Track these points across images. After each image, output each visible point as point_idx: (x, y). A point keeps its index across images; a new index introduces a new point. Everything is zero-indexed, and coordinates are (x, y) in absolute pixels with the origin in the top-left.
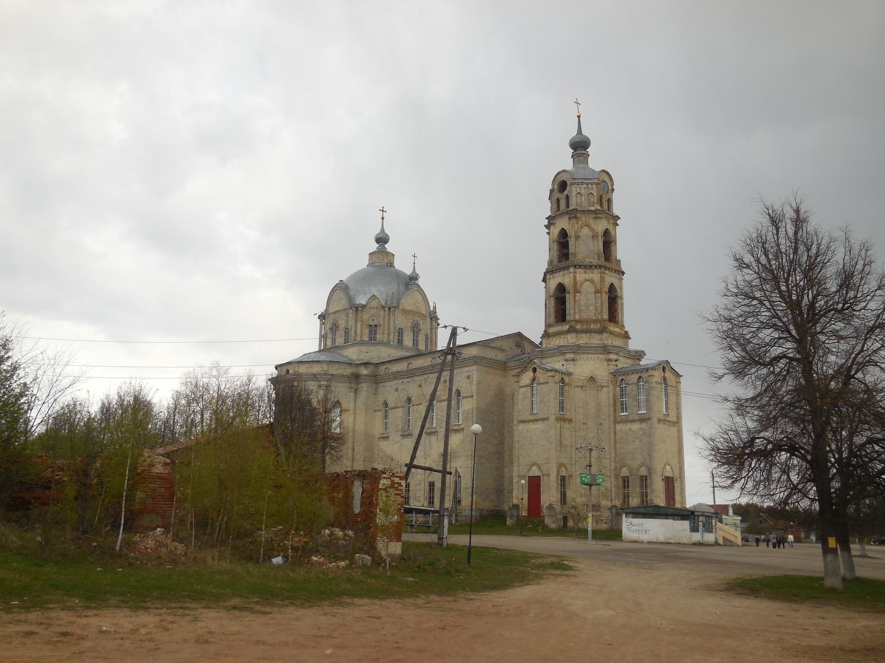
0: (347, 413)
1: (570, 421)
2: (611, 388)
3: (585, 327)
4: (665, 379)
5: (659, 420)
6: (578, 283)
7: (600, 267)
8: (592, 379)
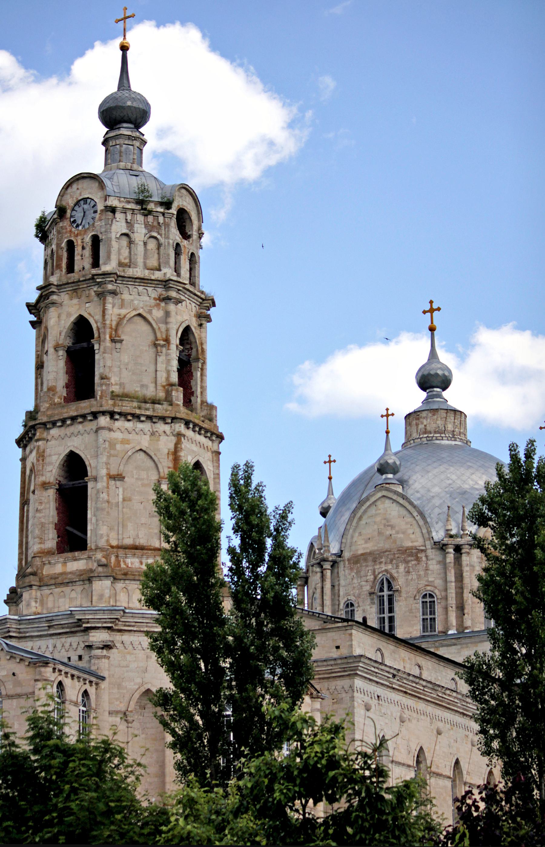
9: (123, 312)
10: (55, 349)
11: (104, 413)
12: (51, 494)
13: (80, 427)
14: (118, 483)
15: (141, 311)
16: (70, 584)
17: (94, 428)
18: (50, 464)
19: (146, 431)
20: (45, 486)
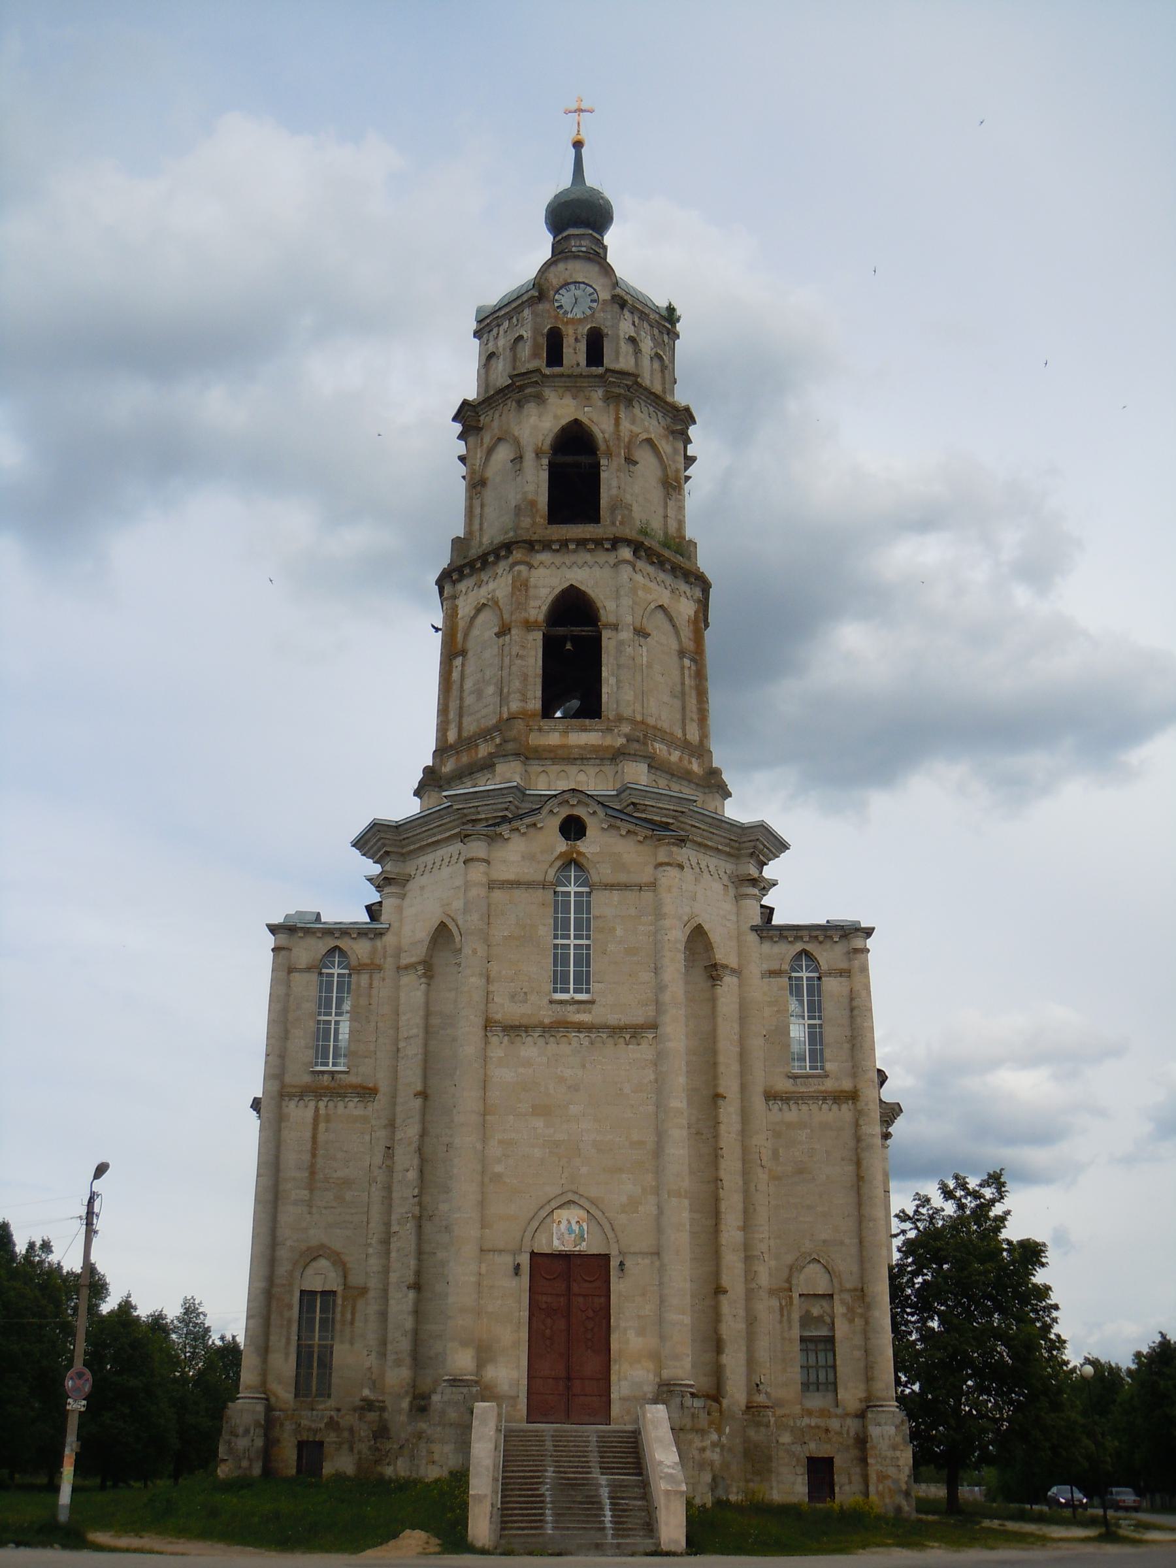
1: (367, 1093)
3: (465, 759)
4: (572, 863)
5: (515, 1030)
6: (462, 624)
9: (636, 429)
11: (628, 542)
12: (536, 639)
13: (588, 557)
14: (642, 639)
15: (653, 436)
16: (579, 762)
18: (536, 598)
19: (668, 582)
20: (528, 626)
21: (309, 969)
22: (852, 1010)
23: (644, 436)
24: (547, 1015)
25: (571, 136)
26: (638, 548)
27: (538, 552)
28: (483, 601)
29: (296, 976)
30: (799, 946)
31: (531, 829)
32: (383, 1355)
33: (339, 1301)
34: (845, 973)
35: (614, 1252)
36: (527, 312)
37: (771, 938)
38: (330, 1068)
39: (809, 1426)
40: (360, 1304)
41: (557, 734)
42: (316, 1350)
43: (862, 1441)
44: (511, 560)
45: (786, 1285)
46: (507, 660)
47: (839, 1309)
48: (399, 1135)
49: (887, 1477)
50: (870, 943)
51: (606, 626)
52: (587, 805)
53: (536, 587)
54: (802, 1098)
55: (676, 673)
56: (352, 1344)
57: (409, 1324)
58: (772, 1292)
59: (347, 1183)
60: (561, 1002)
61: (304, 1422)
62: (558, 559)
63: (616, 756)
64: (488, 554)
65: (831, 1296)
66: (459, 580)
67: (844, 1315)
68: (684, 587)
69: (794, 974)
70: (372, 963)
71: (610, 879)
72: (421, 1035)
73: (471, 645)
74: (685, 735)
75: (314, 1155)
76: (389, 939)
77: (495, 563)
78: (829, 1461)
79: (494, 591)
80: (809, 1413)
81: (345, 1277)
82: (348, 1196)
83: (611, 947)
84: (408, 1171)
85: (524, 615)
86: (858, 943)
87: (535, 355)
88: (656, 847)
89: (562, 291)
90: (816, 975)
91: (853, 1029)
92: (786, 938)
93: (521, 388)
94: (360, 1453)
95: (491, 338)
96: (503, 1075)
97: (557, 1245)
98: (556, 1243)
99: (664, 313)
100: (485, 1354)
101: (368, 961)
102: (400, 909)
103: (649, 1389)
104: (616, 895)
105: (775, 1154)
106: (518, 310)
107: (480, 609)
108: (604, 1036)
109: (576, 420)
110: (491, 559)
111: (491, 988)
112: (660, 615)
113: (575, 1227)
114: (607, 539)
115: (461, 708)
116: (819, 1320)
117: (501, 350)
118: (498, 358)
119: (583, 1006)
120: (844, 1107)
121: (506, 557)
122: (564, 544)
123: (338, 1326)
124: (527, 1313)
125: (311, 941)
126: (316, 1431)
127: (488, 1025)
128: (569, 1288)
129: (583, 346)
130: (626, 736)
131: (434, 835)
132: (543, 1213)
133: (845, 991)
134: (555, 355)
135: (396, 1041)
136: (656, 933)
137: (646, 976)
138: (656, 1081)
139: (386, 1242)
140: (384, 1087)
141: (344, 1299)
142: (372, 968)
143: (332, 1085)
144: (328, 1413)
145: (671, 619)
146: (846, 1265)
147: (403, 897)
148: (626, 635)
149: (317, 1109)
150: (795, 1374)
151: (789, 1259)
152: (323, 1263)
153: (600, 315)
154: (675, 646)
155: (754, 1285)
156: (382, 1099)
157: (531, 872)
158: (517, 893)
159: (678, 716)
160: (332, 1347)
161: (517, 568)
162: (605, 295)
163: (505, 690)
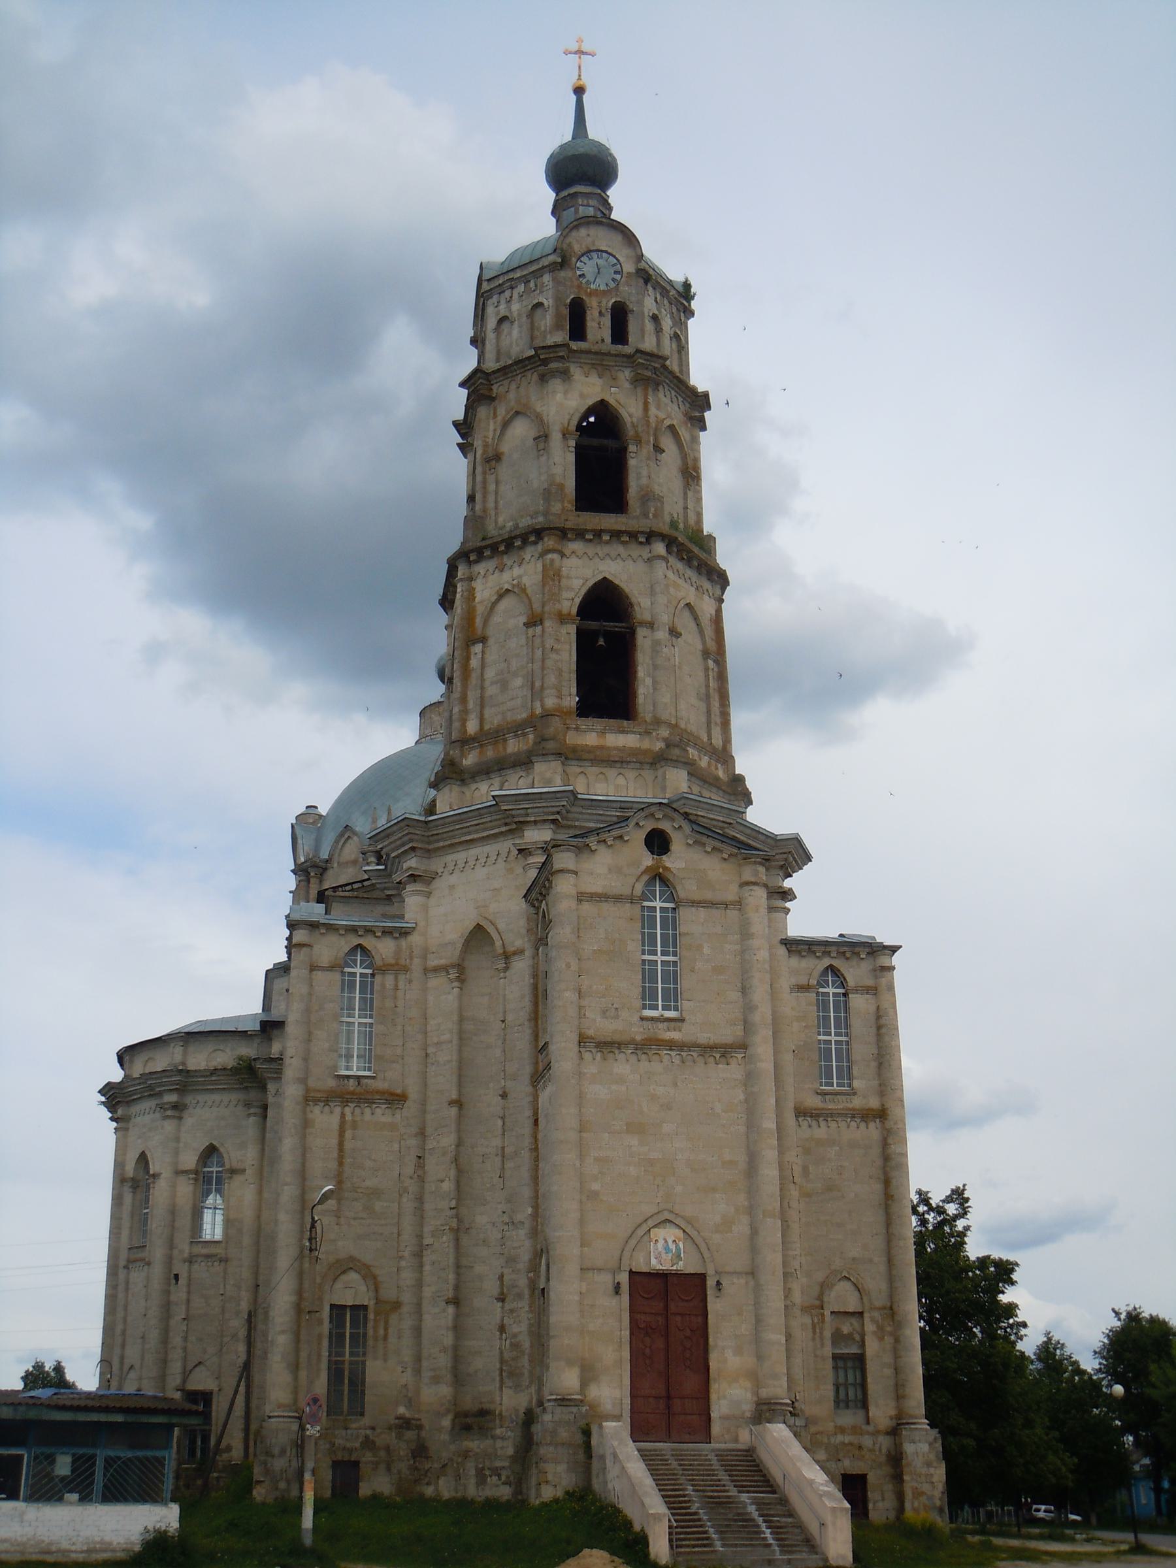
0: (238, 1179)
1: (395, 1099)
2: (528, 953)
3: (490, 753)
4: (659, 878)
5: (608, 1046)
6: (480, 610)
7: (539, 533)
8: (478, 936)
9: (662, 415)
10: (564, 435)
12: (569, 632)
13: (621, 549)
16: (618, 765)
17: (646, 555)
18: (569, 589)
19: (694, 580)
20: (562, 619)
21: (331, 968)
22: (879, 1028)
23: (667, 422)
24: (638, 1032)
25: (572, 81)
26: (671, 543)
27: (570, 540)
28: (506, 586)
29: (319, 975)
30: (827, 962)
31: (617, 842)
32: (418, 1372)
33: (371, 1316)
34: (872, 991)
35: (710, 1272)
36: (547, 278)
37: (799, 952)
38: (354, 1072)
39: (843, 1443)
40: (393, 1319)
41: (594, 735)
42: (347, 1366)
43: (896, 1460)
44: (540, 547)
45: (817, 1303)
46: (539, 653)
47: (870, 1327)
48: (430, 1144)
49: (923, 1493)
50: (896, 960)
51: (641, 624)
52: (673, 820)
53: (568, 577)
54: (832, 1115)
55: (701, 674)
56: (385, 1360)
57: (449, 1340)
58: (805, 1310)
59: (376, 1193)
60: (652, 1019)
61: (338, 1442)
62: (591, 549)
63: (657, 760)
64: (516, 537)
65: (861, 1314)
66: (477, 562)
67: (874, 1333)
68: (707, 585)
69: (821, 990)
70: (397, 964)
71: (697, 897)
72: (455, 1041)
73: (491, 631)
74: (710, 738)
75: (341, 1164)
76: (415, 939)
77: (520, 548)
78: (862, 1478)
79: (520, 577)
80: (841, 1430)
81: (377, 1290)
82: (378, 1206)
83: (699, 965)
84: (442, 1181)
85: (558, 606)
86: (883, 961)
87: (558, 326)
88: (740, 865)
89: (584, 259)
90: (842, 991)
91: (879, 1048)
92: (814, 952)
93: (545, 362)
94: (399, 1472)
95: (503, 301)
96: (598, 1091)
97: (655, 1265)
98: (654, 1262)
99: (681, 289)
100: (588, 1374)
101: (393, 961)
102: (425, 908)
103: (748, 1408)
104: (702, 913)
105: (805, 1171)
106: (538, 273)
107: (502, 594)
108: (695, 1054)
109: (602, 401)
110: (518, 543)
111: (584, 1003)
112: (687, 613)
113: (672, 1246)
114: (642, 533)
115: (482, 698)
116: (849, 1337)
117: (515, 314)
118: (512, 323)
119: (672, 1024)
120: (872, 1125)
121: (535, 543)
122: (598, 534)
123: (370, 1342)
124: (628, 1333)
125: (332, 938)
126: (351, 1451)
127: (582, 1040)
128: (666, 1308)
129: (607, 321)
130: (665, 740)
131: (470, 833)
132: (640, 1232)
133: (872, 1009)
134: (578, 329)
135: (425, 1048)
136: (743, 952)
137: (735, 995)
138: (746, 1101)
139: (419, 1254)
140: (413, 1093)
141: (377, 1313)
142: (397, 968)
143: (359, 1089)
144: (362, 1432)
145: (696, 618)
146: (876, 1284)
147: (428, 895)
148: (662, 634)
149: (343, 1115)
150: (828, 1391)
151: (820, 1276)
152: (353, 1276)
153: (624, 289)
154: (700, 647)
155: (788, 1303)
156: (411, 1108)
157: (619, 885)
158: (605, 906)
159: (703, 719)
160: (364, 1363)
161: (550, 556)
162: (629, 267)
163: (538, 684)
